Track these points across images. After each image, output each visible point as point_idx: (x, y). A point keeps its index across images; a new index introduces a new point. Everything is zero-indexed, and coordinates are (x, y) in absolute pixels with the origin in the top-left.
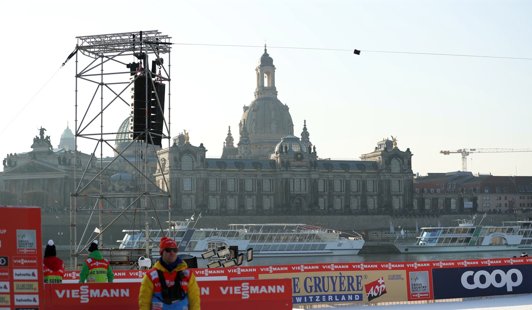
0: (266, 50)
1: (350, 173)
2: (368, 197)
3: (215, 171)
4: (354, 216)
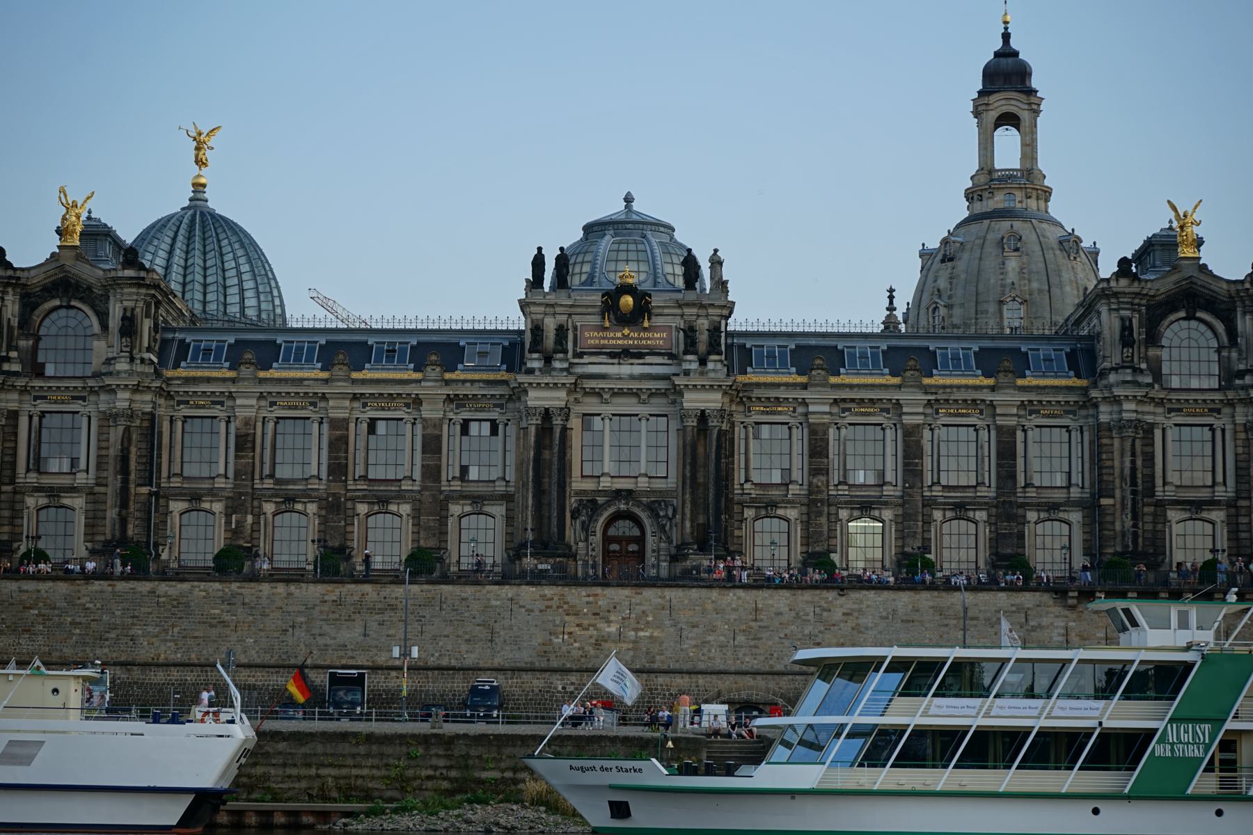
0: (1006, 37)
1: (926, 390)
2: (1032, 516)
3: (209, 380)
4: (831, 595)
